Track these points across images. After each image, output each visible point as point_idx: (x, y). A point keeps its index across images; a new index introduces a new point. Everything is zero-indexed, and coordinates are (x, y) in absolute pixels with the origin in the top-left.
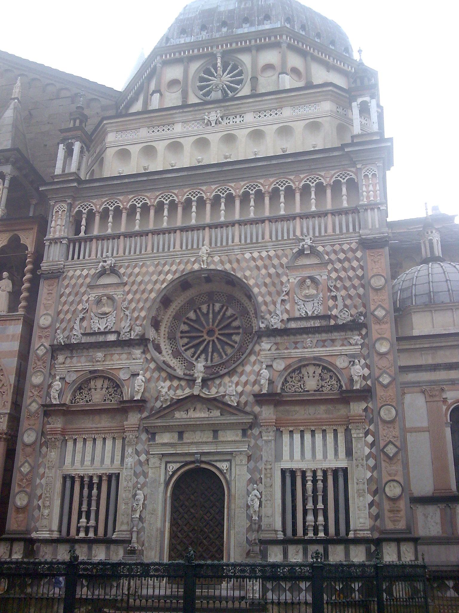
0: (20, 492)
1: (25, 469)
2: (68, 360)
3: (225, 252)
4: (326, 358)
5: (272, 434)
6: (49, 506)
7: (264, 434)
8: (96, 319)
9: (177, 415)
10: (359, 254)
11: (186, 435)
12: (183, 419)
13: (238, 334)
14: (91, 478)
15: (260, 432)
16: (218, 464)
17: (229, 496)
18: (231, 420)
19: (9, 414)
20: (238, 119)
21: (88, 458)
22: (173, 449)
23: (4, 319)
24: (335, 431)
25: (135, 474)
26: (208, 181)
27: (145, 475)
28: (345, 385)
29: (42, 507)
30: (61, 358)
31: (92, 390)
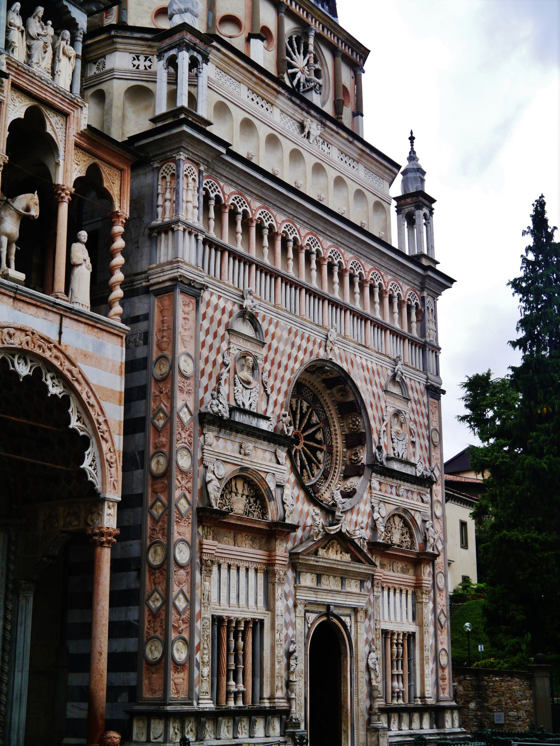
0: (176, 639)
1: (181, 604)
2: (215, 442)
3: (344, 345)
4: (410, 511)
5: (380, 589)
6: (208, 662)
7: (375, 589)
8: (240, 386)
9: (321, 552)
10: (425, 399)
11: (324, 580)
12: (330, 559)
13: (321, 450)
14: (238, 622)
15: (373, 585)
16: (343, 618)
17: (351, 657)
18: (362, 568)
19: (119, 504)
20: (325, 147)
21: (233, 595)
22: (314, 596)
23: (102, 327)
24: (407, 591)
25: (287, 625)
26: (328, 233)
27: (294, 625)
28: (419, 544)
29: (201, 664)
30: (210, 436)
31: (233, 494)
